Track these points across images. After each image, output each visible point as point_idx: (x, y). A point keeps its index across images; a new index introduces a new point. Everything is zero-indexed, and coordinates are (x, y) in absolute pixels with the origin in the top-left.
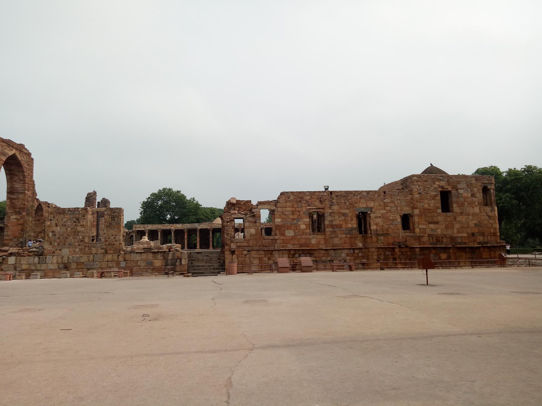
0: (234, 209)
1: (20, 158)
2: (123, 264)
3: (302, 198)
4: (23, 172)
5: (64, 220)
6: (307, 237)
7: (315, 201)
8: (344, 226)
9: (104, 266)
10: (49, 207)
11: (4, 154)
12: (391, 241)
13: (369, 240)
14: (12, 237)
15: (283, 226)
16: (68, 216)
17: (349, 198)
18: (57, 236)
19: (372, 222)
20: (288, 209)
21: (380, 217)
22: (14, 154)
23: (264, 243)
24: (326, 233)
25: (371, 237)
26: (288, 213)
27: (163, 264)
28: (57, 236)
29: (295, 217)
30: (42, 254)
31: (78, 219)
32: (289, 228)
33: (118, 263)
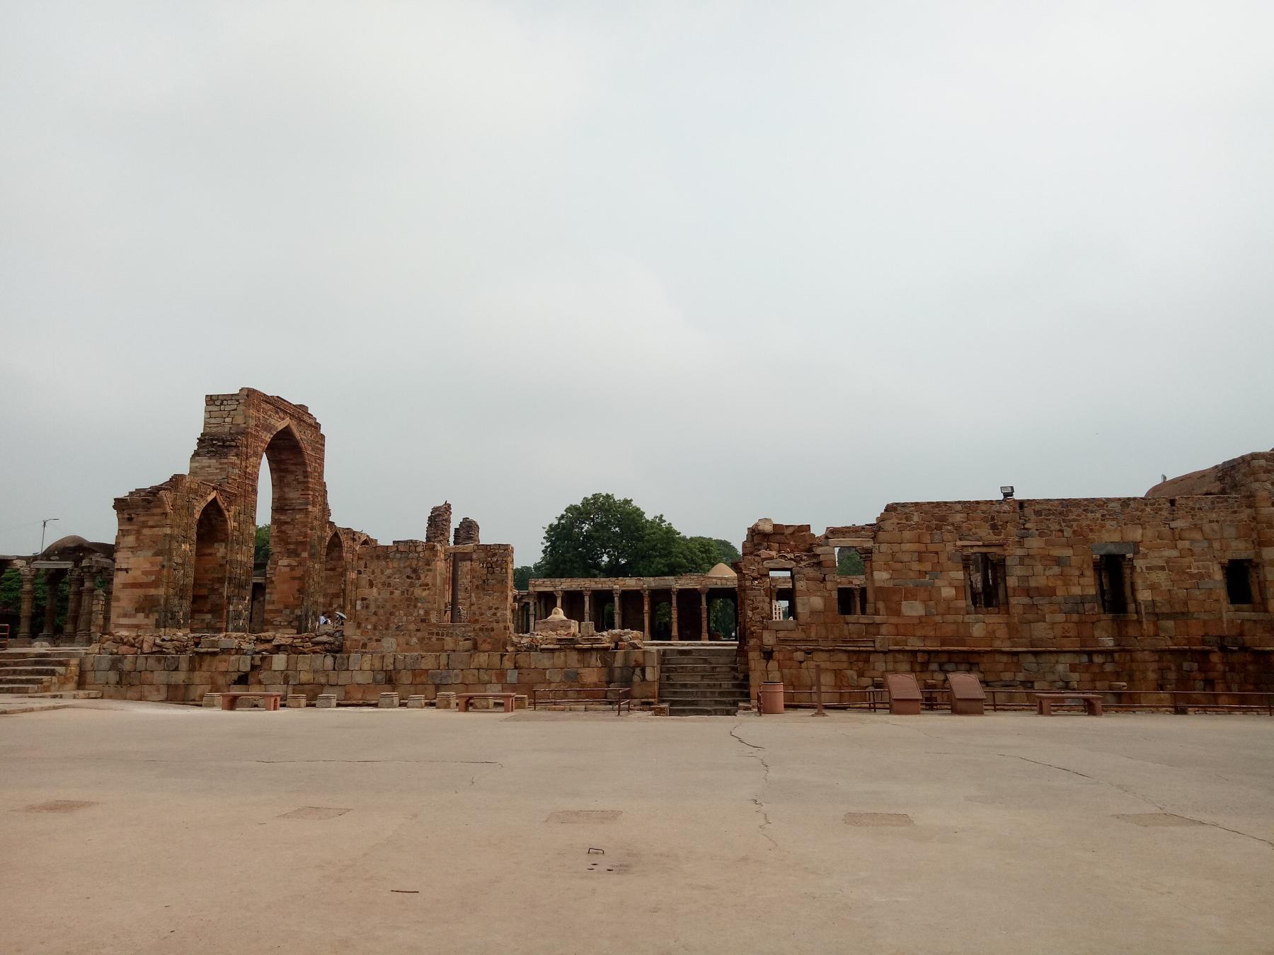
0: (768, 548)
1: (297, 435)
2: (512, 676)
3: (943, 519)
4: (304, 464)
5: (388, 572)
6: (959, 619)
9: (471, 679)
10: (354, 540)
11: (268, 428)
12: (1197, 632)
13: (1132, 631)
14: (281, 606)
15: (895, 590)
16: (395, 565)
18: (373, 608)
19: (1139, 582)
21: (1163, 568)
22: (288, 427)
23: (846, 632)
24: (1012, 611)
25: (1140, 622)
26: (906, 558)
27: (604, 679)
28: (373, 608)
29: (927, 566)
30: (340, 649)
31: (415, 571)
32: (910, 595)
33: (502, 674)
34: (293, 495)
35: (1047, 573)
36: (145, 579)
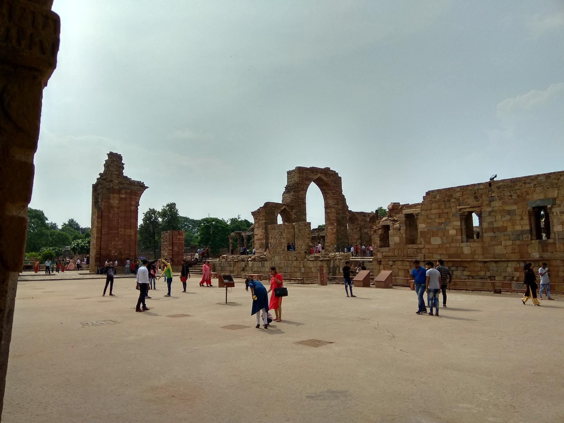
6: (458, 245)
7: (468, 198)
8: (509, 229)
17: (516, 188)
19: (555, 220)
20: (434, 211)
25: (554, 243)
26: (433, 217)
29: (443, 220)
32: (435, 234)
33: (300, 270)
34: (331, 202)
35: (503, 219)
36: (260, 238)
